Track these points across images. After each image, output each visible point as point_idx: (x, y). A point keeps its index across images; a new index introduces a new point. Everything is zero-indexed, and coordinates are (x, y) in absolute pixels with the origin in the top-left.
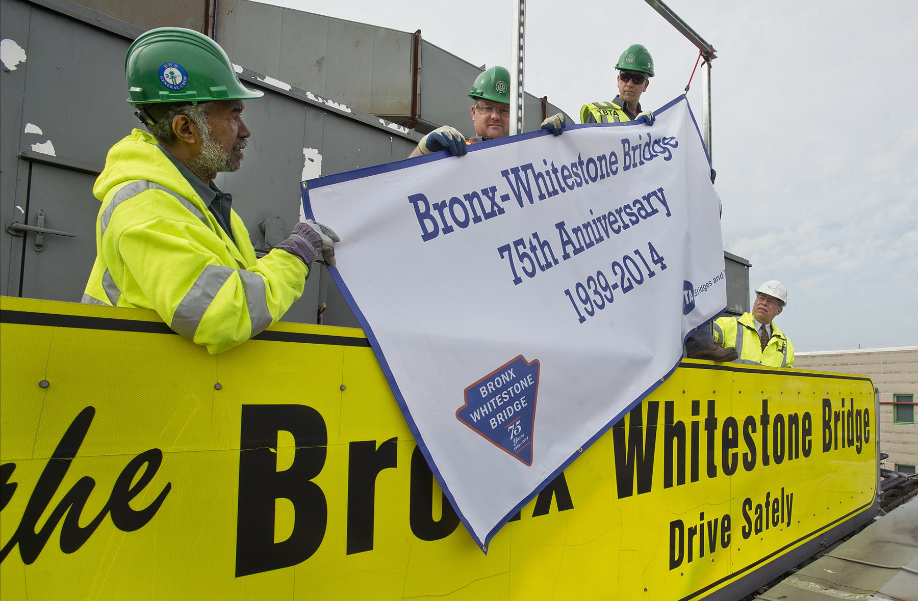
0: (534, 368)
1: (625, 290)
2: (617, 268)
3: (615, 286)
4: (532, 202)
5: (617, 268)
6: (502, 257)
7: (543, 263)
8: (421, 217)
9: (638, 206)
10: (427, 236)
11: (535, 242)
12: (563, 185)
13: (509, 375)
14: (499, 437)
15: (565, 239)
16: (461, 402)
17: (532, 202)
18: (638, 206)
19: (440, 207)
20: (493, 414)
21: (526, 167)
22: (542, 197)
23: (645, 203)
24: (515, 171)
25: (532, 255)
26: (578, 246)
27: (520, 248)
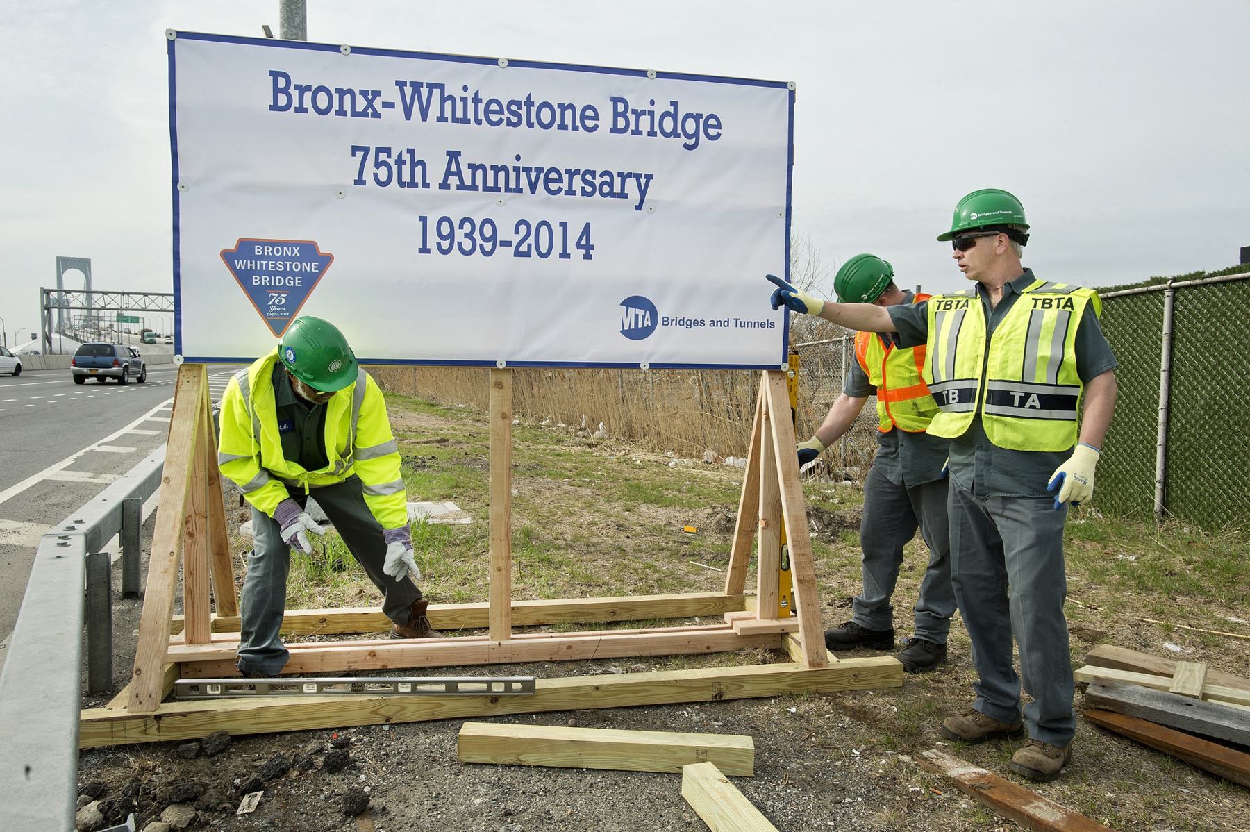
0: (325, 261)
1: (517, 254)
2: (523, 229)
3: (506, 244)
4: (424, 118)
5: (523, 229)
6: (354, 155)
7: (406, 178)
8: (277, 90)
9: (607, 178)
10: (275, 107)
11: (406, 157)
12: (481, 116)
13: (293, 251)
14: (259, 296)
15: (453, 168)
16: (232, 246)
17: (424, 118)
18: (607, 178)
19: (302, 90)
20: (260, 273)
21: (431, 86)
22: (442, 118)
23: (617, 181)
24: (416, 86)
25: (395, 168)
26: (468, 182)
27: (383, 157)
